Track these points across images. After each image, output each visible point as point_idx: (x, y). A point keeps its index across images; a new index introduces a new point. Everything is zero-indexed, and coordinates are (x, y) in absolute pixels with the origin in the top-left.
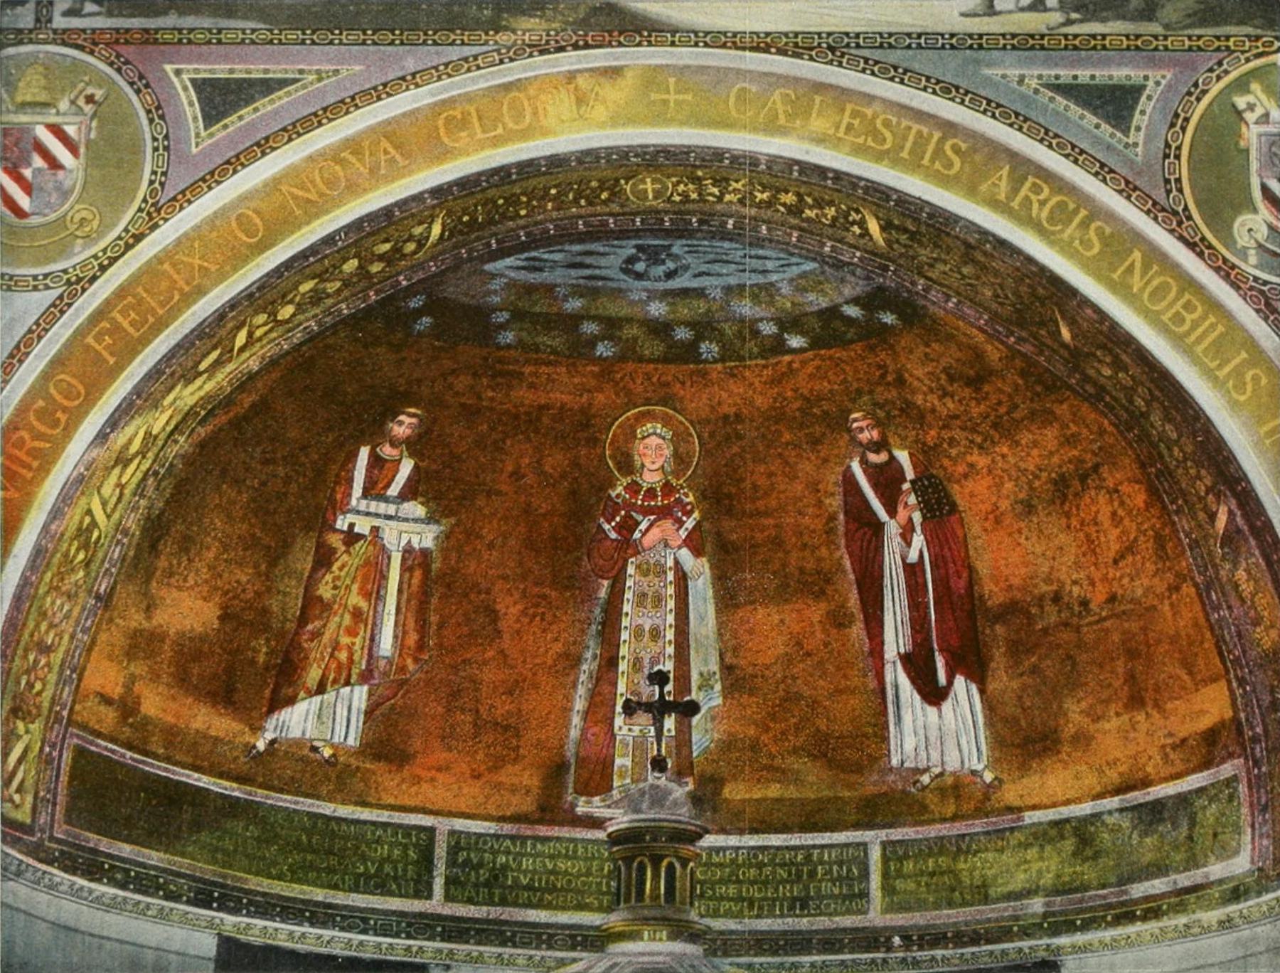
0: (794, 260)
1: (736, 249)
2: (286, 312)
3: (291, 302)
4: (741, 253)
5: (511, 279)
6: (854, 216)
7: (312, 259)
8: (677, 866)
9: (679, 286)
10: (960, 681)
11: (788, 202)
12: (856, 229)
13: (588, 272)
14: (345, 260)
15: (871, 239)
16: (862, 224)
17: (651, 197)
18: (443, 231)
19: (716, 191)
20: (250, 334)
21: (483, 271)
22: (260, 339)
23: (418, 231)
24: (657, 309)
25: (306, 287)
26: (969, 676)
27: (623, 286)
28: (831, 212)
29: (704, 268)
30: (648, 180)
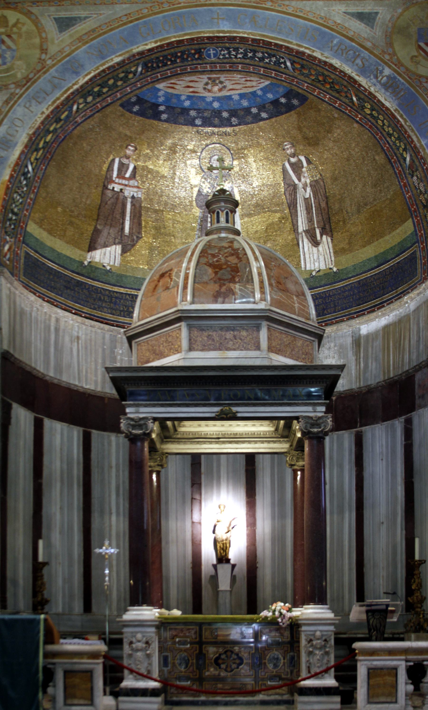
0: (262, 81)
1: (242, 78)
2: (90, 99)
3: (91, 95)
4: (244, 79)
5: (166, 92)
6: (282, 60)
7: (98, 78)
8: (220, 212)
9: (223, 95)
10: (324, 237)
11: (259, 56)
12: (283, 66)
13: (191, 90)
14: (109, 79)
15: (288, 69)
16: (285, 63)
17: (212, 57)
18: (142, 71)
19: (234, 53)
20: (78, 108)
21: (156, 87)
22: (81, 109)
23: (133, 70)
24: (216, 105)
25: (96, 89)
26: (327, 234)
27: (204, 95)
28: (274, 59)
29: (231, 87)
30: (211, 49)
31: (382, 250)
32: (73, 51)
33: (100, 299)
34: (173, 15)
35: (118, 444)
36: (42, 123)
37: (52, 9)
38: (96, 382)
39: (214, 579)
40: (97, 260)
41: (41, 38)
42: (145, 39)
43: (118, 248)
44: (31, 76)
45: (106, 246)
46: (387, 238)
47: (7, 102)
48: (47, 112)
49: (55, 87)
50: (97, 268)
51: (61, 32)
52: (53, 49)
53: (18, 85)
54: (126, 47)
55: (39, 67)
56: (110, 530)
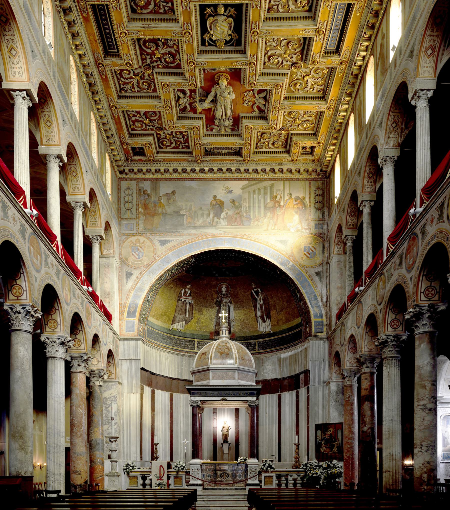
31: (290, 327)
32: (167, 254)
33: (176, 343)
34: (207, 240)
35: (183, 398)
36: (155, 282)
37: (158, 237)
38: (175, 374)
39: (222, 448)
40: (175, 327)
41: (153, 248)
42: (196, 250)
43: (184, 323)
44: (150, 263)
45: (178, 322)
46: (292, 322)
47: (140, 273)
48: (157, 278)
49: (160, 268)
50: (175, 331)
51: (162, 246)
52: (158, 253)
53: (145, 267)
54: (188, 253)
55: (153, 260)
56: (181, 431)
